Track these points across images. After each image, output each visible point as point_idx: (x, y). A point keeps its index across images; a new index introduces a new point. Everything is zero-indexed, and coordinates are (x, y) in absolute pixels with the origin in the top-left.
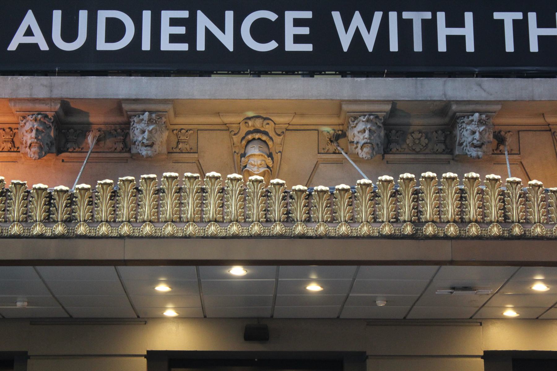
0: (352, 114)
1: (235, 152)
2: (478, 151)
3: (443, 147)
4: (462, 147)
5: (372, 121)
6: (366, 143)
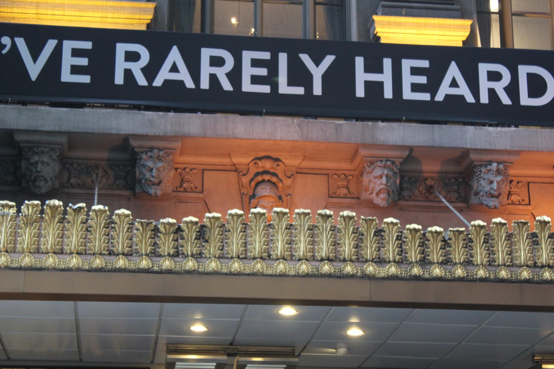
0: (369, 159)
1: (243, 193)
2: (495, 201)
3: (456, 195)
4: (478, 196)
5: (388, 166)
6: (383, 189)
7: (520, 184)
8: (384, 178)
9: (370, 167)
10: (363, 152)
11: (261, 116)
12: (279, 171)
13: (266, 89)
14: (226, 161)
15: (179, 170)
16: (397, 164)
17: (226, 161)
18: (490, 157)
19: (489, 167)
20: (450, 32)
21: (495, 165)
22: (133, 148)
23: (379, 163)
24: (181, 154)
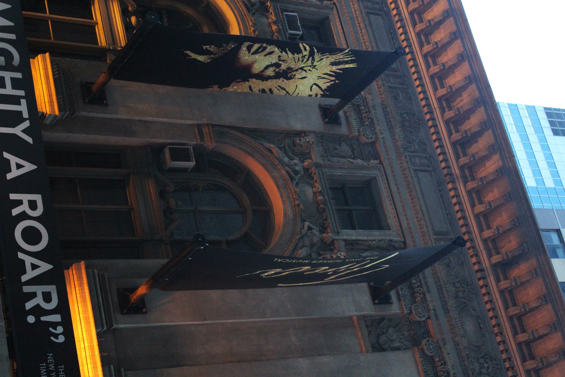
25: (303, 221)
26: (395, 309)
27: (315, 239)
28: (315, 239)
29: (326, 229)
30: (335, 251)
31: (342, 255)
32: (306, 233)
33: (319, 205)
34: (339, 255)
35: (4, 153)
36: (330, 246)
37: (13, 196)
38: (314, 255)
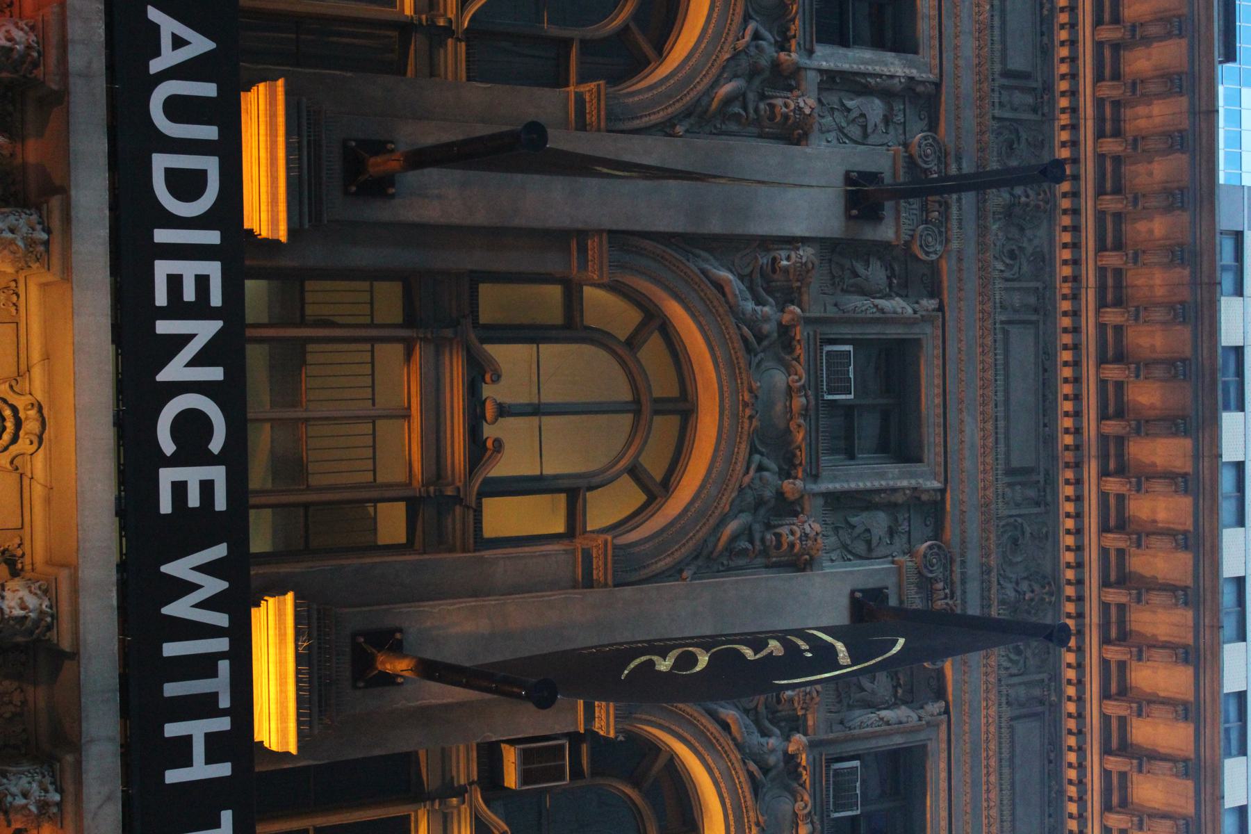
7: (13, 310)
8: (22, 613)
9: (40, 588)
10: (64, 574)
11: (113, 342)
12: (23, 445)
13: (161, 299)
14: (36, 355)
15: (13, 284)
16: (48, 634)
17: (36, 355)
18: (70, 788)
19: (51, 788)
20: (265, 210)
21: (57, 798)
22: (47, 202)
23: (46, 603)
24: (44, 286)
25: (747, 18)
26: (886, 232)
27: (764, 62)
28: (764, 62)
29: (795, 466)
30: (796, 93)
31: (808, 103)
32: (748, 47)
33: (791, 418)
34: (808, 530)
35: (150, 8)
36: (785, 79)
37: (166, 506)
38: (751, 96)
